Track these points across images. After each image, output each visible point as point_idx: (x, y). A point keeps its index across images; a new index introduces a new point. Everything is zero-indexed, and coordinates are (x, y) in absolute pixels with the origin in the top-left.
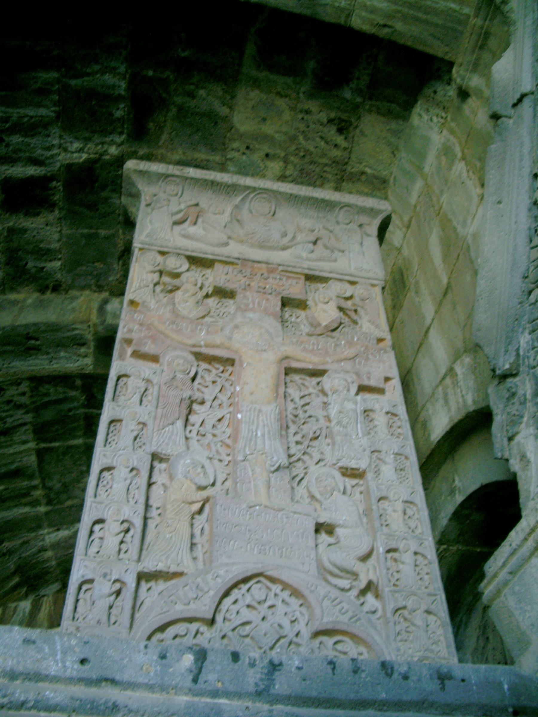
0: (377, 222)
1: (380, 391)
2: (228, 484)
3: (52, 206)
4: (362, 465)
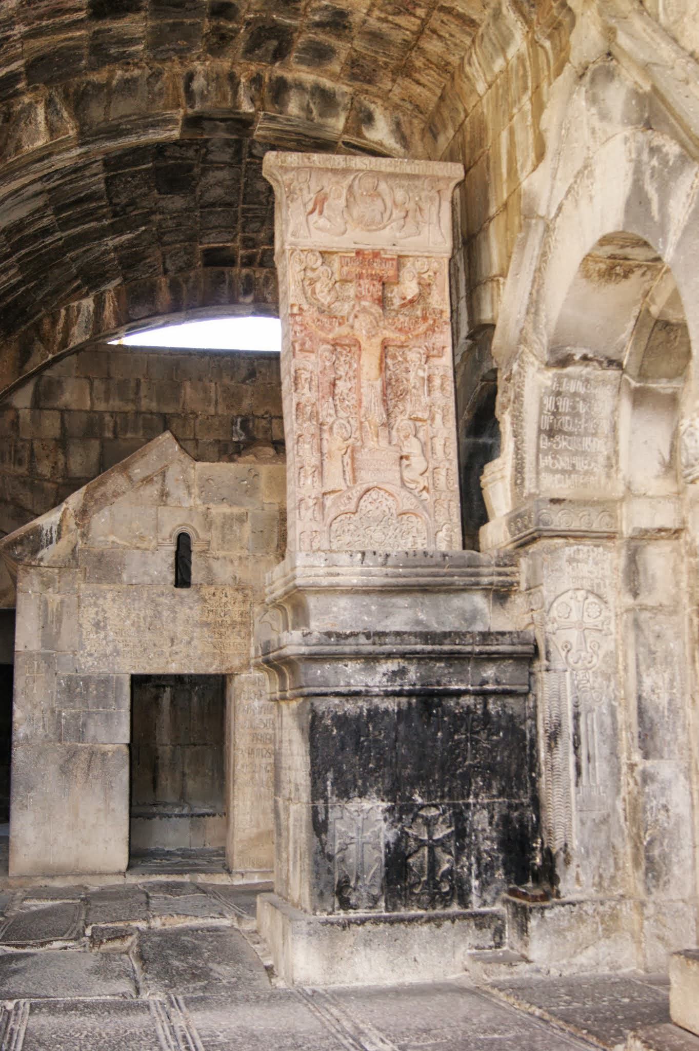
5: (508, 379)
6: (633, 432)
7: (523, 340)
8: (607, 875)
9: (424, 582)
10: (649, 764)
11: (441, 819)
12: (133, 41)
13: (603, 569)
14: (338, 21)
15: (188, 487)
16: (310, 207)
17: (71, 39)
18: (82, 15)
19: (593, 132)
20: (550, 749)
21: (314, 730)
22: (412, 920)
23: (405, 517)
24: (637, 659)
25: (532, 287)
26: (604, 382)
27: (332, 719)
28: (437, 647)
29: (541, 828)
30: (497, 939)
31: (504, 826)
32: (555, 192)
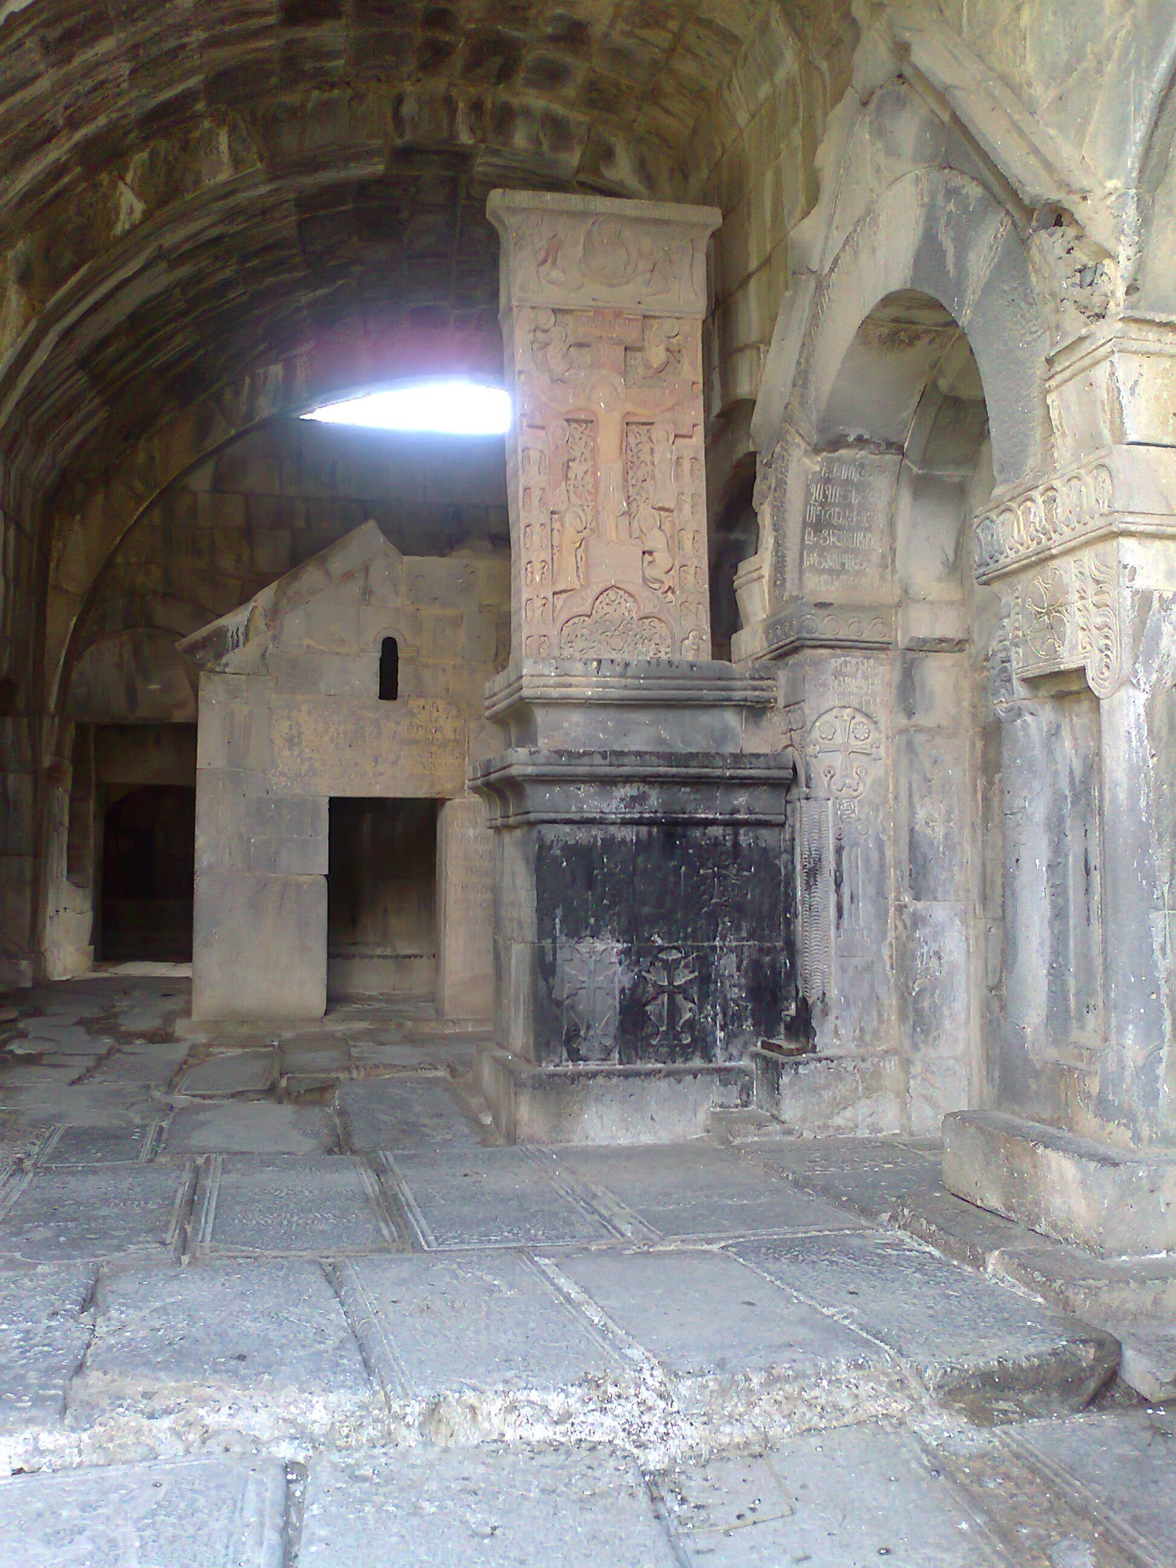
0: (709, 232)
1: (691, 437)
2: (594, 523)
3: (338, 15)
4: (672, 506)
5: (768, 465)
6: (914, 526)
7: (788, 418)
8: (869, 1028)
9: (667, 696)
10: (919, 905)
11: (683, 963)
12: (332, 55)
13: (873, 684)
14: (574, 34)
15: (395, 586)
16: (542, 255)
17: (258, 50)
18: (272, 20)
19: (878, 170)
20: (808, 887)
21: (542, 863)
22: (649, 1074)
23: (647, 621)
24: (910, 787)
25: (801, 354)
26: (881, 469)
27: (562, 849)
28: (682, 770)
29: (796, 975)
30: (744, 1097)
31: (755, 972)
32: (830, 242)
